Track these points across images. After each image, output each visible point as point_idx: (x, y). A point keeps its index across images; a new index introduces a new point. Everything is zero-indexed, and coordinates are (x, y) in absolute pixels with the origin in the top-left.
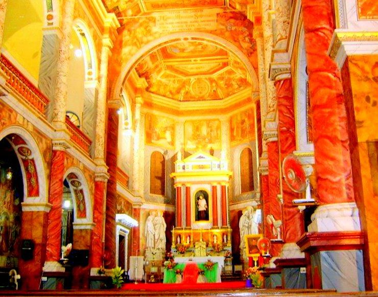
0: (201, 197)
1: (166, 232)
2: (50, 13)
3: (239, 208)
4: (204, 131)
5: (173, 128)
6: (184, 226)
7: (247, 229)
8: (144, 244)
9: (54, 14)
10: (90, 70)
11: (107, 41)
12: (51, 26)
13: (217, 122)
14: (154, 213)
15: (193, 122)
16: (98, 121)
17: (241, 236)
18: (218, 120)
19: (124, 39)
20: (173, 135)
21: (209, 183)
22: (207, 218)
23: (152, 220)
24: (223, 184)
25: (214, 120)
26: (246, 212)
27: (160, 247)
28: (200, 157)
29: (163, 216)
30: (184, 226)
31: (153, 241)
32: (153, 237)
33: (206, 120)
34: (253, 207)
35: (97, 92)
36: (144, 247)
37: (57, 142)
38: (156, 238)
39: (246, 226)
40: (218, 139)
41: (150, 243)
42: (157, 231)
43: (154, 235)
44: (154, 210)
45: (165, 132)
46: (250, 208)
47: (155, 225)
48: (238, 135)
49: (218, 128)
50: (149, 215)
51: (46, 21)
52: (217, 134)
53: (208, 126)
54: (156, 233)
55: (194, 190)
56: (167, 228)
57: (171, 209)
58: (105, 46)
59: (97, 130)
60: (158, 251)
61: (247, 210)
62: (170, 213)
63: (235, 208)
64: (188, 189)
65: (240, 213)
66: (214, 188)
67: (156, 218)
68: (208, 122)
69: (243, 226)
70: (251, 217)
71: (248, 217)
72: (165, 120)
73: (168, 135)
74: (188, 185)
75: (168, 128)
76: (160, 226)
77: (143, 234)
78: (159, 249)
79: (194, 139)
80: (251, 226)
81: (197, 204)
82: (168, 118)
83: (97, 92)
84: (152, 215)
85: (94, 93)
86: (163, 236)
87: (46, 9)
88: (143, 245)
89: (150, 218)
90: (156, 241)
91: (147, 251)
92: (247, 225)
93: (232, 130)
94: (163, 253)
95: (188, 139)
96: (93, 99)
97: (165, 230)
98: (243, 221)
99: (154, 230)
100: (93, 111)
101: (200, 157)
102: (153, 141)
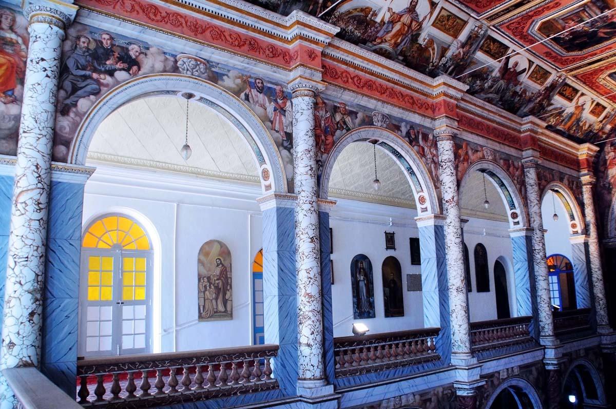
2: (513, 211)
9: (518, 211)
10: (573, 222)
11: (586, 178)
12: (518, 227)
16: (594, 279)
19: (607, 157)
35: (586, 245)
37: (548, 362)
51: (511, 220)
58: (585, 185)
59: (595, 291)
83: (586, 245)
85: (583, 249)
87: (507, 207)
96: (583, 257)
100: (586, 272)
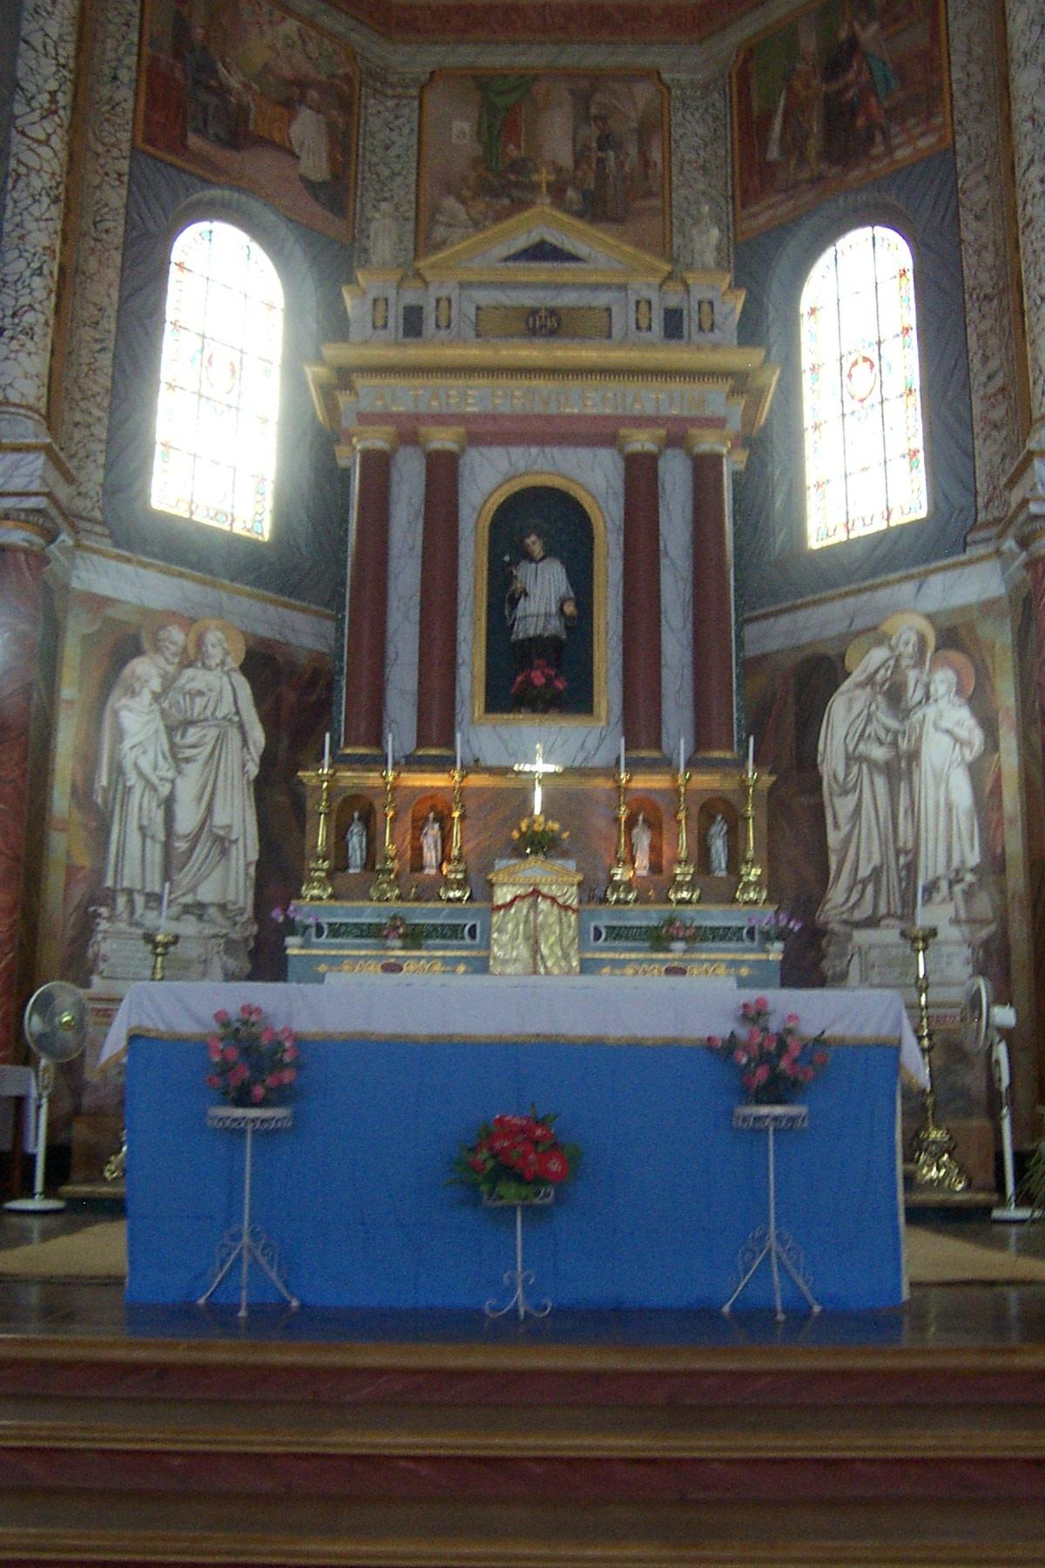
0: (534, 544)
1: (262, 788)
3: (806, 637)
4: (557, 139)
5: (342, 101)
6: (400, 735)
7: (880, 782)
8: (84, 860)
13: (644, 92)
14: (176, 635)
15: (483, 82)
17: (834, 838)
18: (654, 75)
20: (343, 146)
21: (601, 434)
22: (572, 697)
23: (156, 684)
24: (707, 442)
25: (632, 76)
26: (878, 655)
27: (208, 892)
28: (541, 252)
29: (247, 668)
30: (400, 735)
31: (155, 854)
32: (159, 815)
33: (570, 75)
34: (930, 617)
36: (78, 892)
38: (187, 820)
39: (873, 765)
40: (649, 194)
41: (133, 859)
42: (193, 770)
43: (169, 804)
44: (171, 616)
45: (289, 105)
46: (908, 628)
47: (175, 727)
48: (794, 145)
49: (652, 127)
50: (138, 652)
52: (646, 163)
53: (583, 113)
54: (187, 790)
55: (488, 479)
56: (267, 760)
57: (305, 632)
60: (189, 927)
61: (882, 640)
62: (303, 659)
63: (772, 645)
64: (443, 476)
65: (818, 676)
66: (641, 478)
67: (189, 672)
68: (587, 91)
69: (852, 758)
70: (914, 695)
71: (895, 695)
72: (290, 26)
73: (306, 129)
74: (443, 439)
75: (313, 94)
76: (220, 740)
77: (82, 793)
78: (198, 910)
79: (485, 189)
80: (914, 756)
81: (503, 596)
82: (309, 21)
84: (158, 649)
86: (237, 814)
88: (71, 870)
89: (146, 670)
90: (182, 846)
91: (104, 925)
92: (879, 753)
93: (751, 130)
94: (230, 947)
95: (448, 189)
97: (253, 770)
98: (844, 720)
99: (166, 770)
101: (541, 252)
102: (194, 141)
